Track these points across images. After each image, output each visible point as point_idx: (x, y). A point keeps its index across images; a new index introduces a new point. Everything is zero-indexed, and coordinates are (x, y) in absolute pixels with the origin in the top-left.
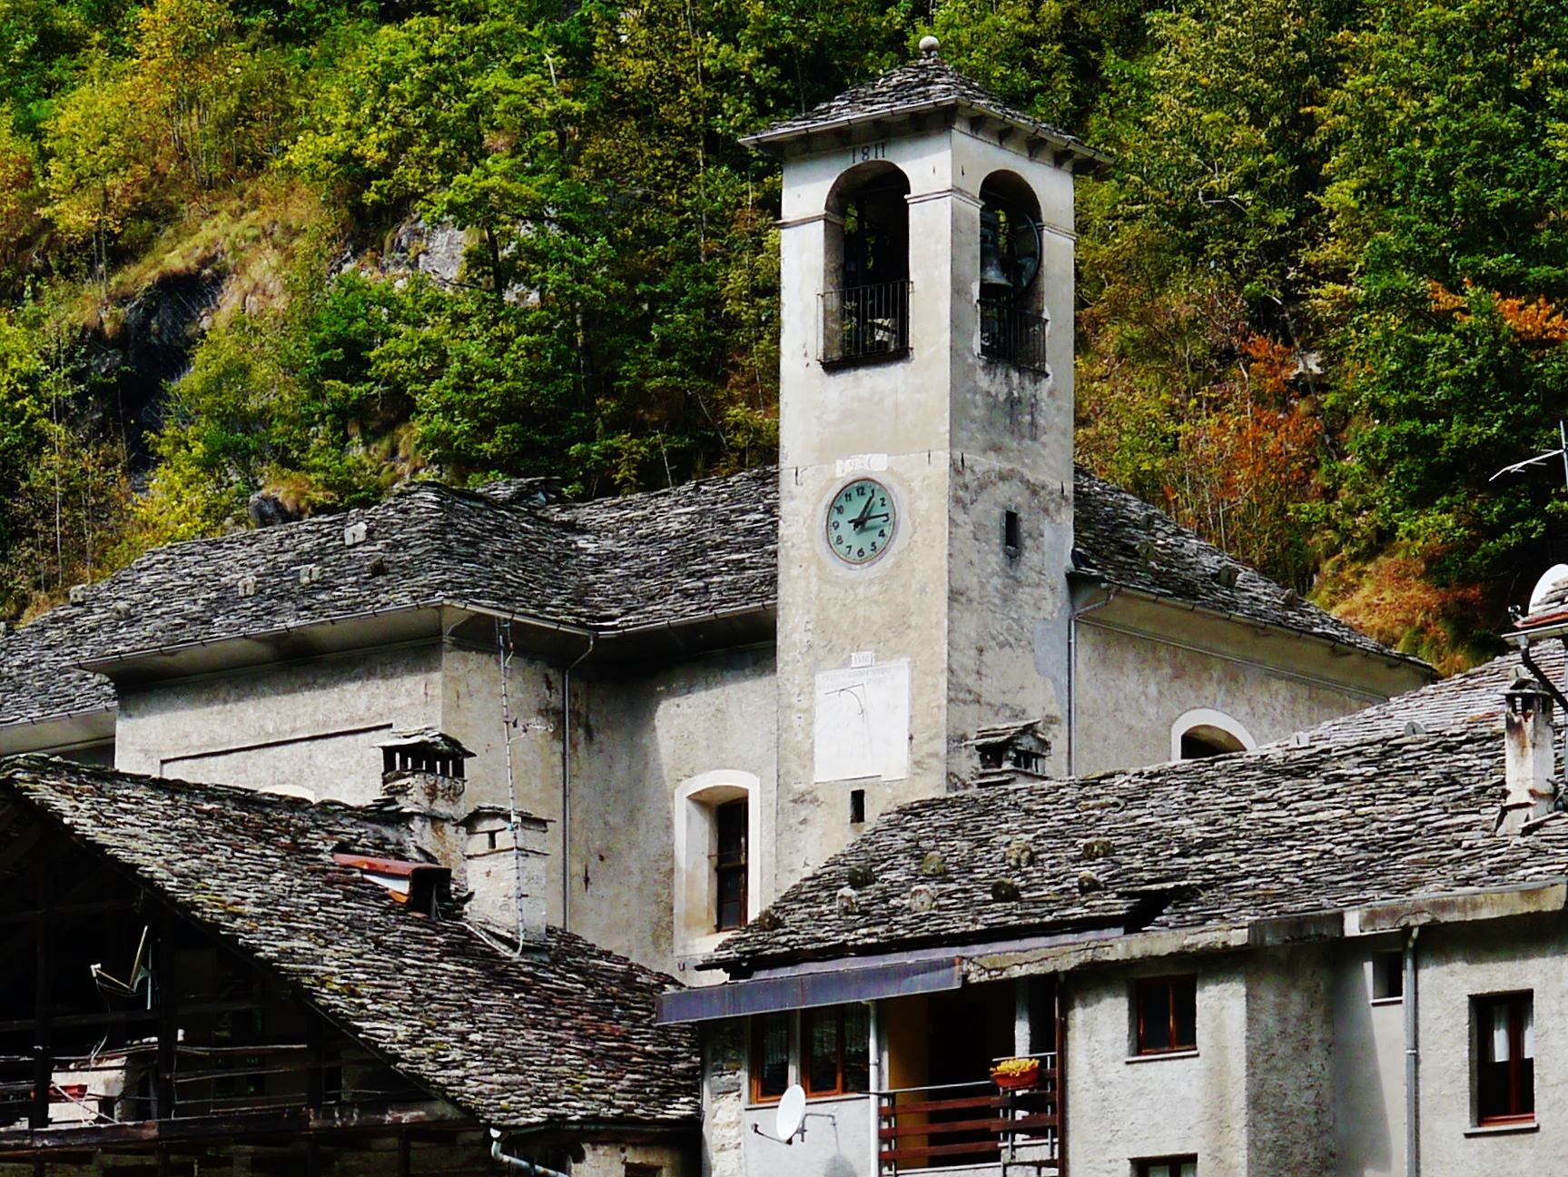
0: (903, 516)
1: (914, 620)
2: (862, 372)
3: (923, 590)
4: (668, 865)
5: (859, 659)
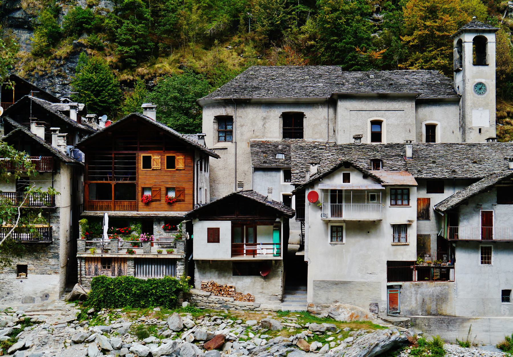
0: (488, 89)
1: (490, 104)
2: (480, 67)
3: (491, 100)
4: (421, 134)
5: (480, 109)
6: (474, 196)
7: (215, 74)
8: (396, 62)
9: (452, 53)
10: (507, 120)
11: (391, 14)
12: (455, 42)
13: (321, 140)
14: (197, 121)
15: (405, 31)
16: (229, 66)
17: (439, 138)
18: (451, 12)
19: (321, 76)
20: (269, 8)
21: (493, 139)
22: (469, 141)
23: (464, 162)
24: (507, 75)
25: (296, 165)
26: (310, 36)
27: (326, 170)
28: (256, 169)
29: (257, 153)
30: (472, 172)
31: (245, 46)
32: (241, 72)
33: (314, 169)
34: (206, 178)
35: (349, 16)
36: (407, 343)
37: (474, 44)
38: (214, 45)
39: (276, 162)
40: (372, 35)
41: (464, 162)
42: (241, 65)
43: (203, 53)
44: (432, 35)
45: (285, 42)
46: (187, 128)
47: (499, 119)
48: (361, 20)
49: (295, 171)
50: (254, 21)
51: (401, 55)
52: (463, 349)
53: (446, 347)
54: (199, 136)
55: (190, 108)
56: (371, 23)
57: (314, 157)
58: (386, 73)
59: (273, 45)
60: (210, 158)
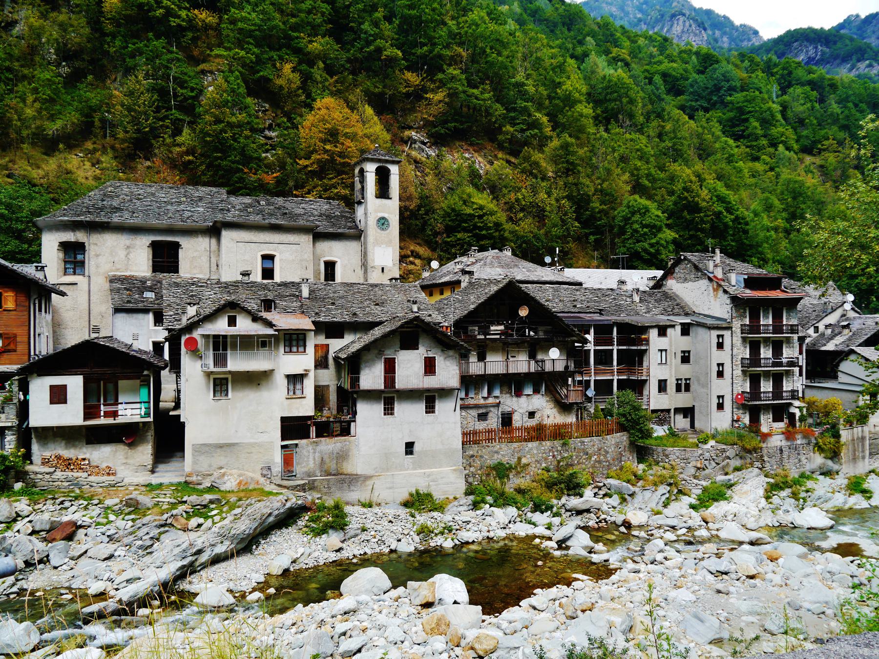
6: (376, 341)
7: (60, 188)
8: (291, 188)
9: (353, 183)
10: (411, 259)
11: (286, 132)
12: (357, 171)
13: (201, 276)
14: (34, 248)
15: (302, 153)
16: (80, 179)
17: (339, 277)
18: (353, 137)
19: (201, 199)
20: (135, 111)
21: (396, 279)
22: (371, 281)
23: (366, 303)
24: (411, 211)
25: (169, 305)
26: (188, 150)
27: (208, 311)
28: (117, 310)
29: (118, 290)
30: (374, 315)
31: (101, 155)
32: (96, 187)
33: (192, 311)
34: (47, 322)
35: (236, 130)
36: (304, 509)
37: (376, 174)
38: (59, 150)
39: (143, 302)
40: (264, 155)
41: (366, 303)
42: (96, 178)
43: (43, 160)
44: (332, 161)
45: (156, 155)
46: (19, 256)
47: (403, 258)
48: (251, 136)
49: (168, 313)
50: (114, 125)
51: (296, 181)
52: (365, 510)
53: (348, 509)
54: (37, 267)
55: (24, 231)
56: (262, 141)
57: (192, 296)
58: (280, 201)
59: (140, 158)
60: (53, 295)
